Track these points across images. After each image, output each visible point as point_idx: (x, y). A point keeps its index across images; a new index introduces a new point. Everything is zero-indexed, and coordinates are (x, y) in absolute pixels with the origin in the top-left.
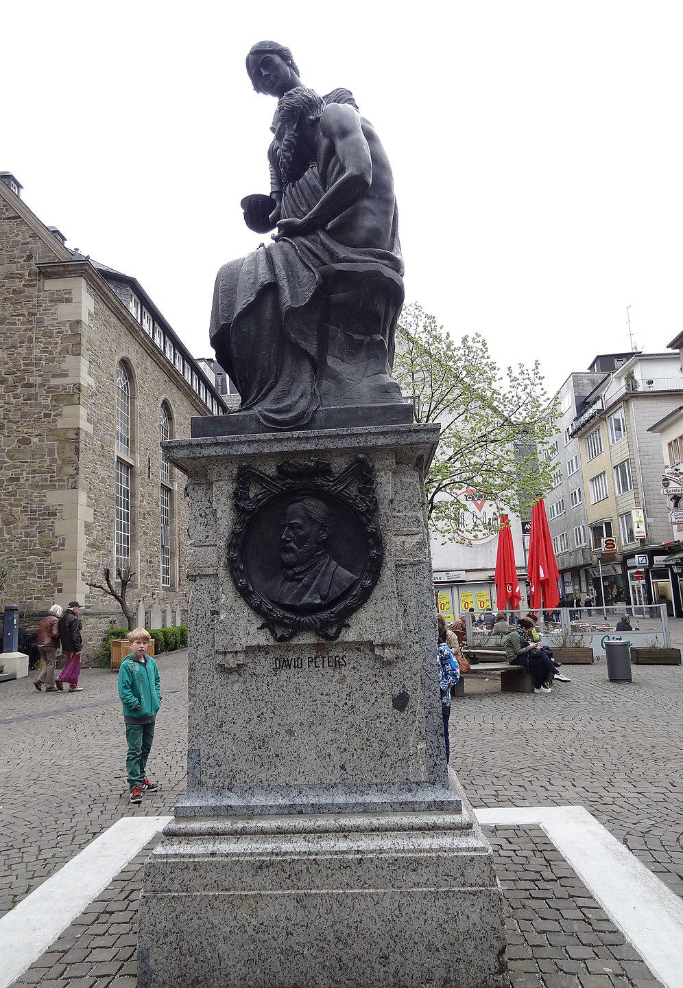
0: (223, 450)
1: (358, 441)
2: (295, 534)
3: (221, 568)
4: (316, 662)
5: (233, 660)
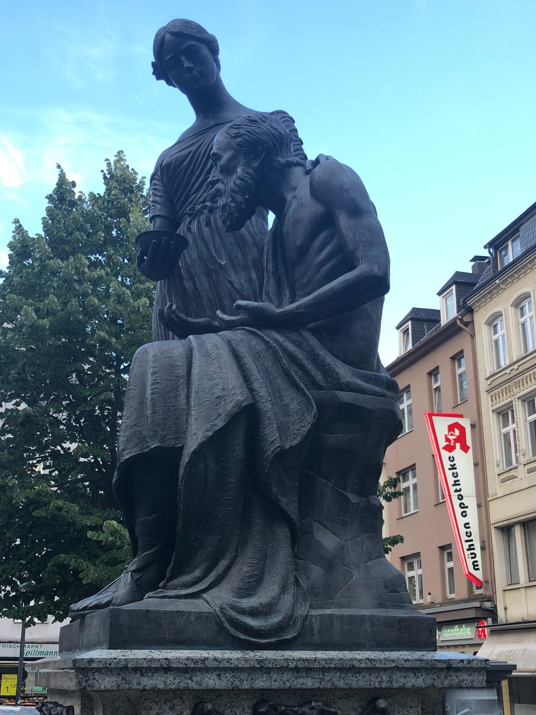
1: (379, 679)
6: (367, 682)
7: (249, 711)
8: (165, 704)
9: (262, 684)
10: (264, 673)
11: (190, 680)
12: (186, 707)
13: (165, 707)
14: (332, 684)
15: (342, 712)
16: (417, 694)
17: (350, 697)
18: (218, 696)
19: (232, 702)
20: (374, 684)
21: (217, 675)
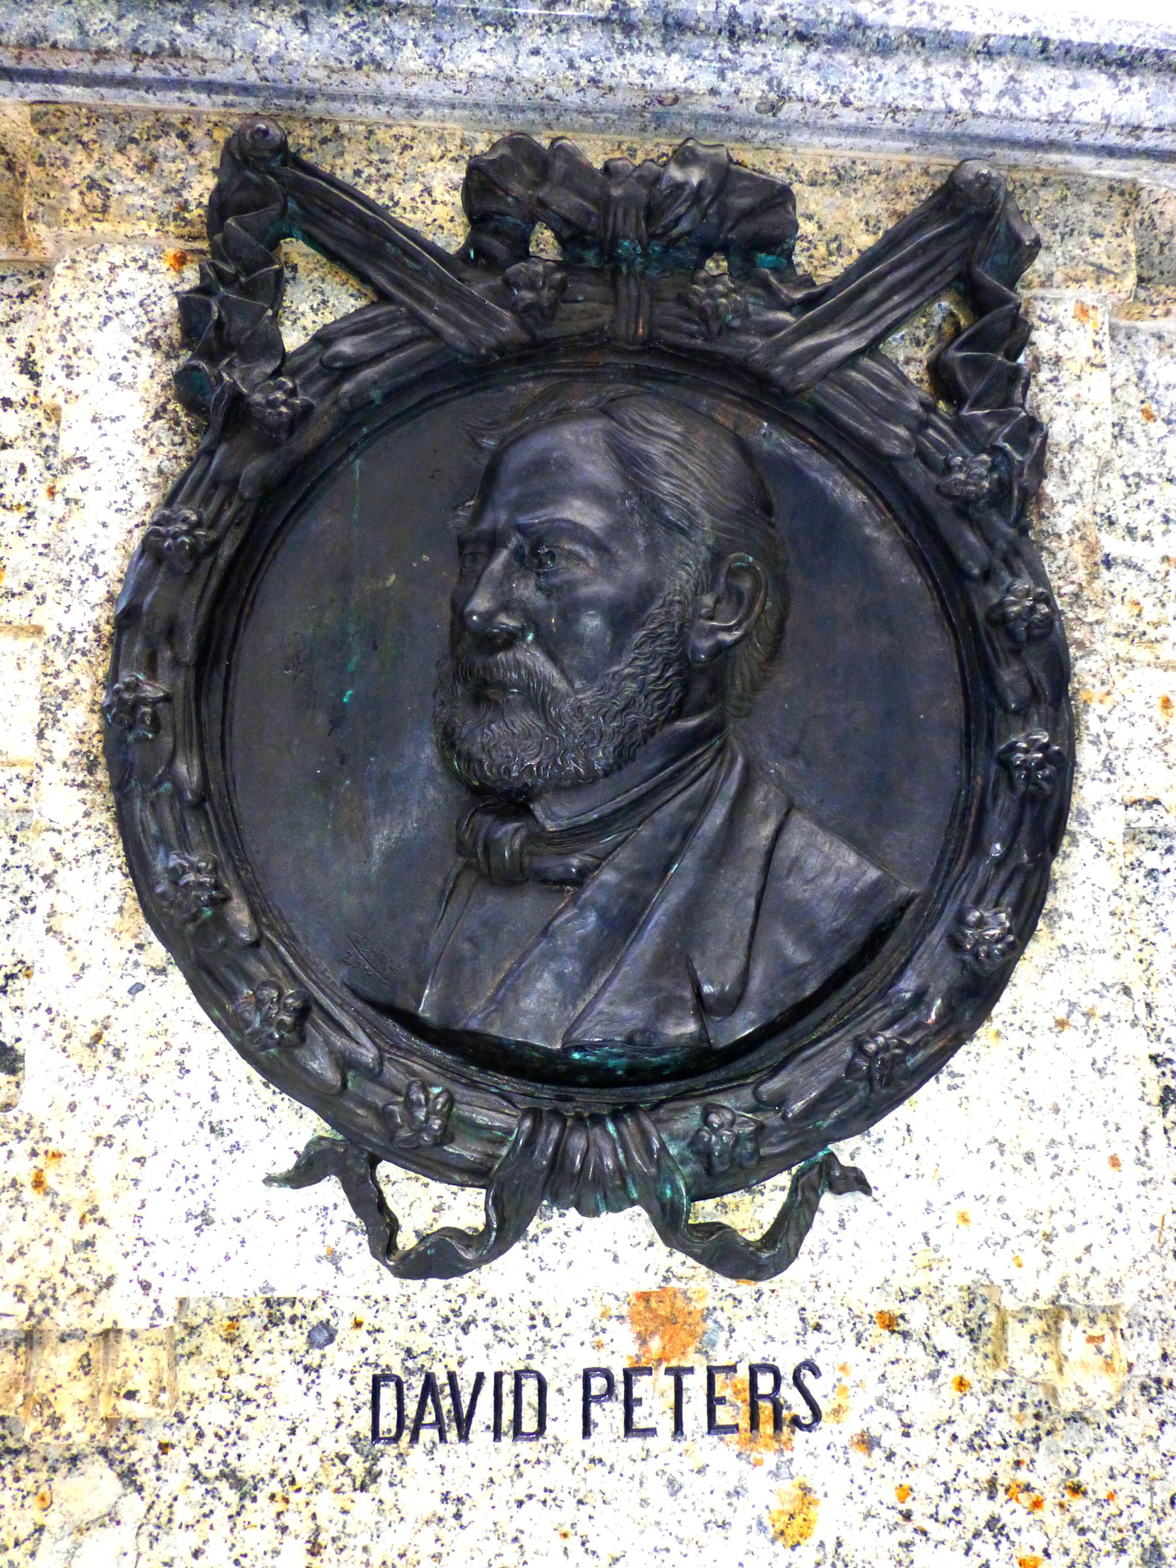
0: (129, 24)
1: (967, 82)
2: (548, 592)
3: (53, 772)
4: (630, 1404)
5: (81, 1389)
6: (915, 87)
7: (447, 198)
8: (121, 150)
9: (479, 58)
10: (489, 24)
11: (183, 23)
12: (201, 165)
13: (120, 160)
14: (769, 82)
15: (820, 227)
16: (1122, 193)
17: (853, 180)
18: (324, 141)
19: (382, 161)
20: (947, 96)
21: (295, 18)
